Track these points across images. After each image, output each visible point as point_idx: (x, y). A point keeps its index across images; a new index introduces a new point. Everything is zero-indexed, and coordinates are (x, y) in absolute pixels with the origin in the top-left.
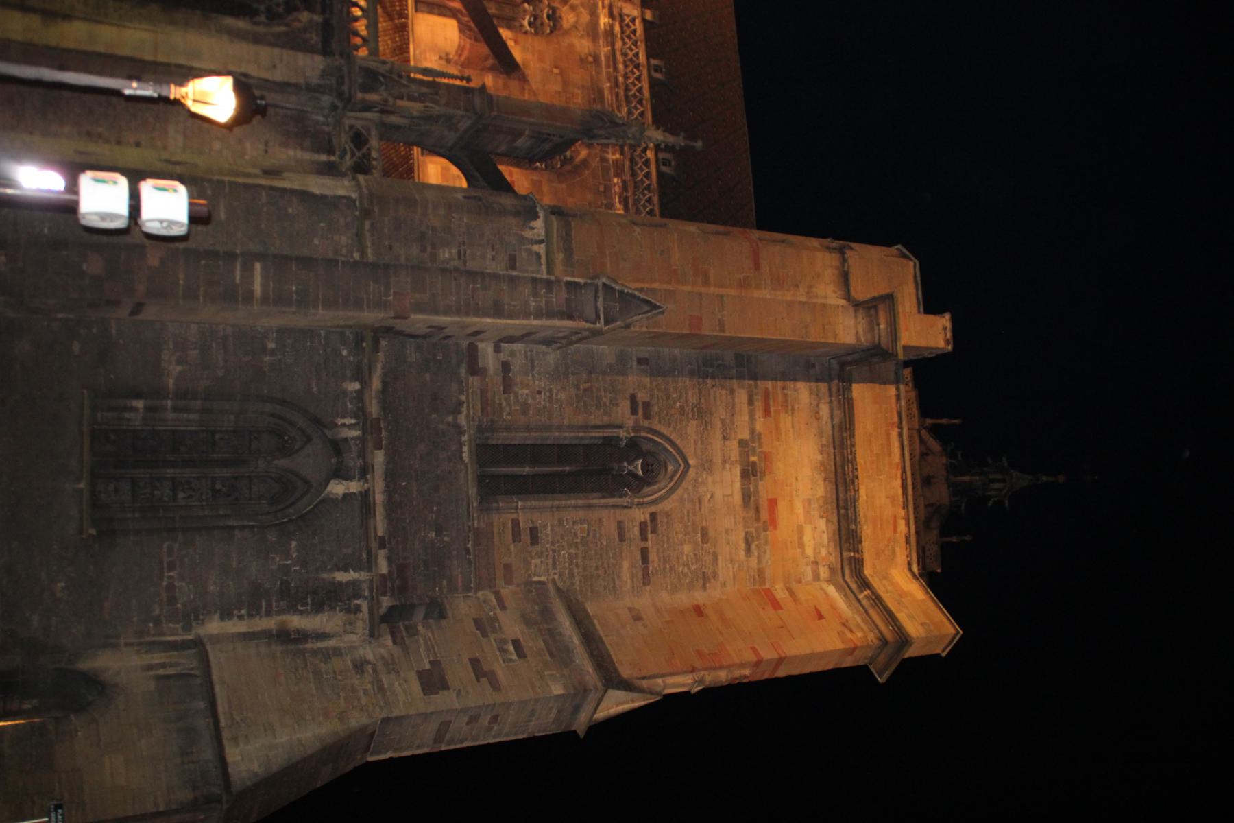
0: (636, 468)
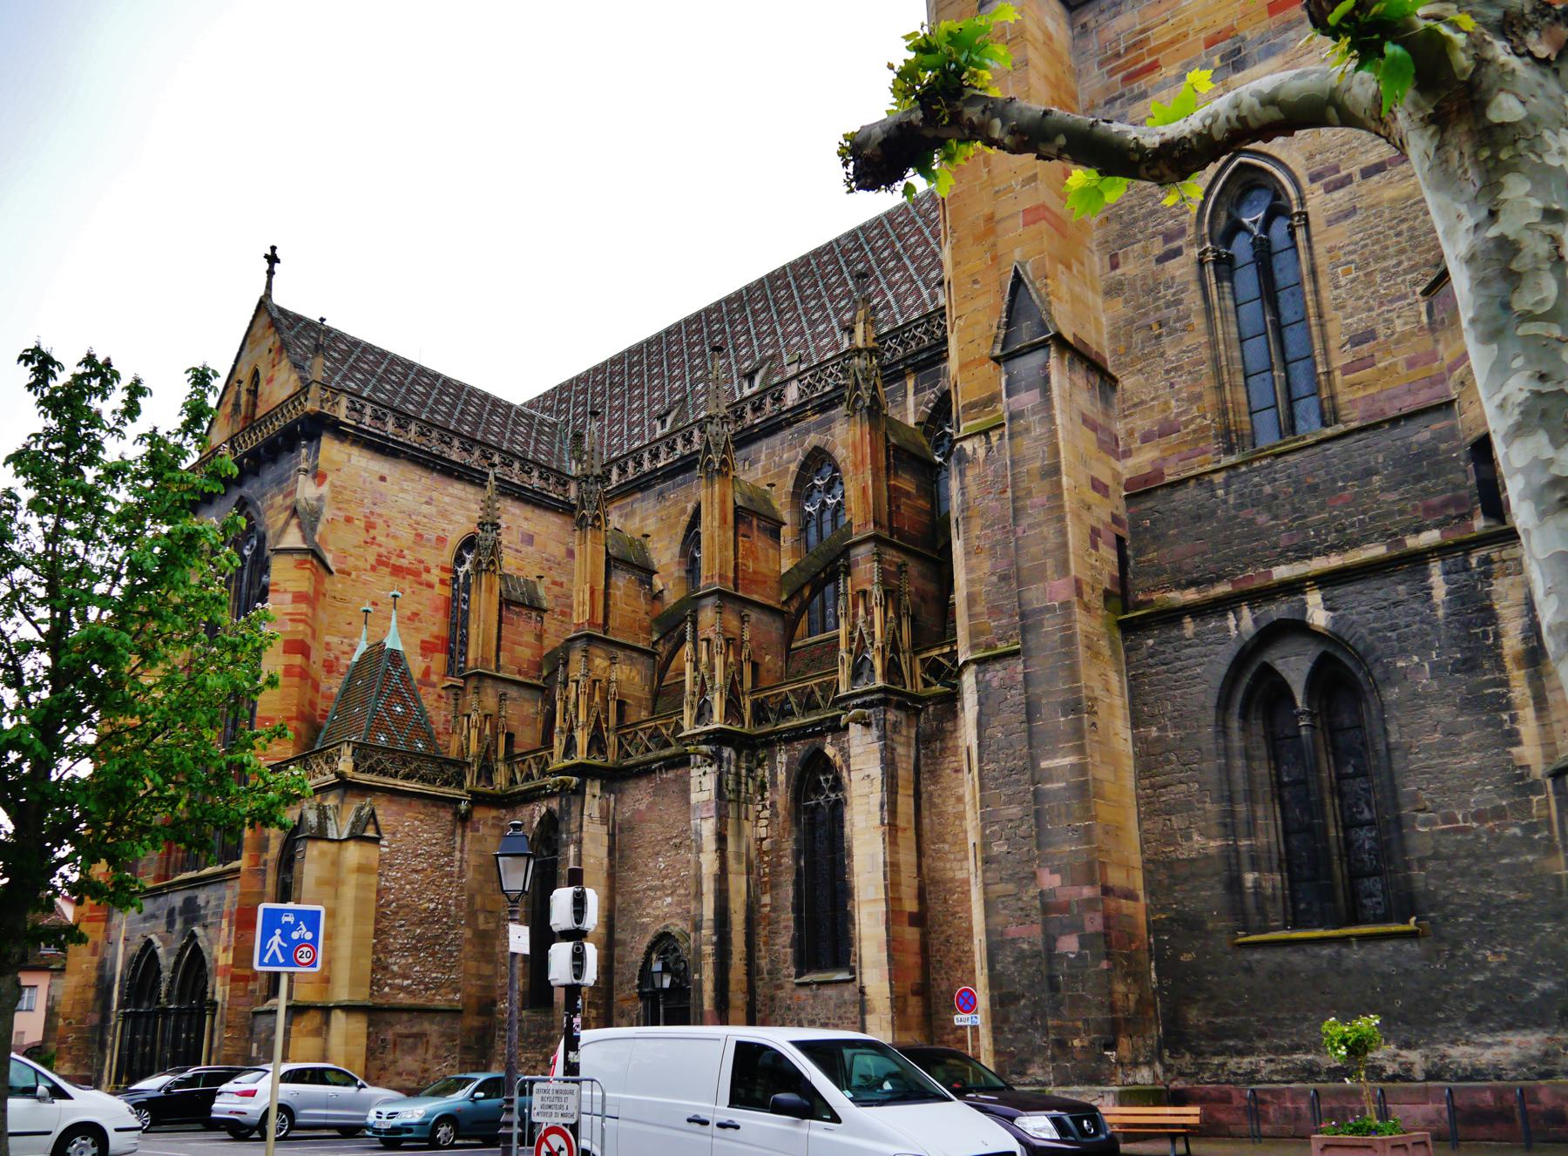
0: (1255, 222)
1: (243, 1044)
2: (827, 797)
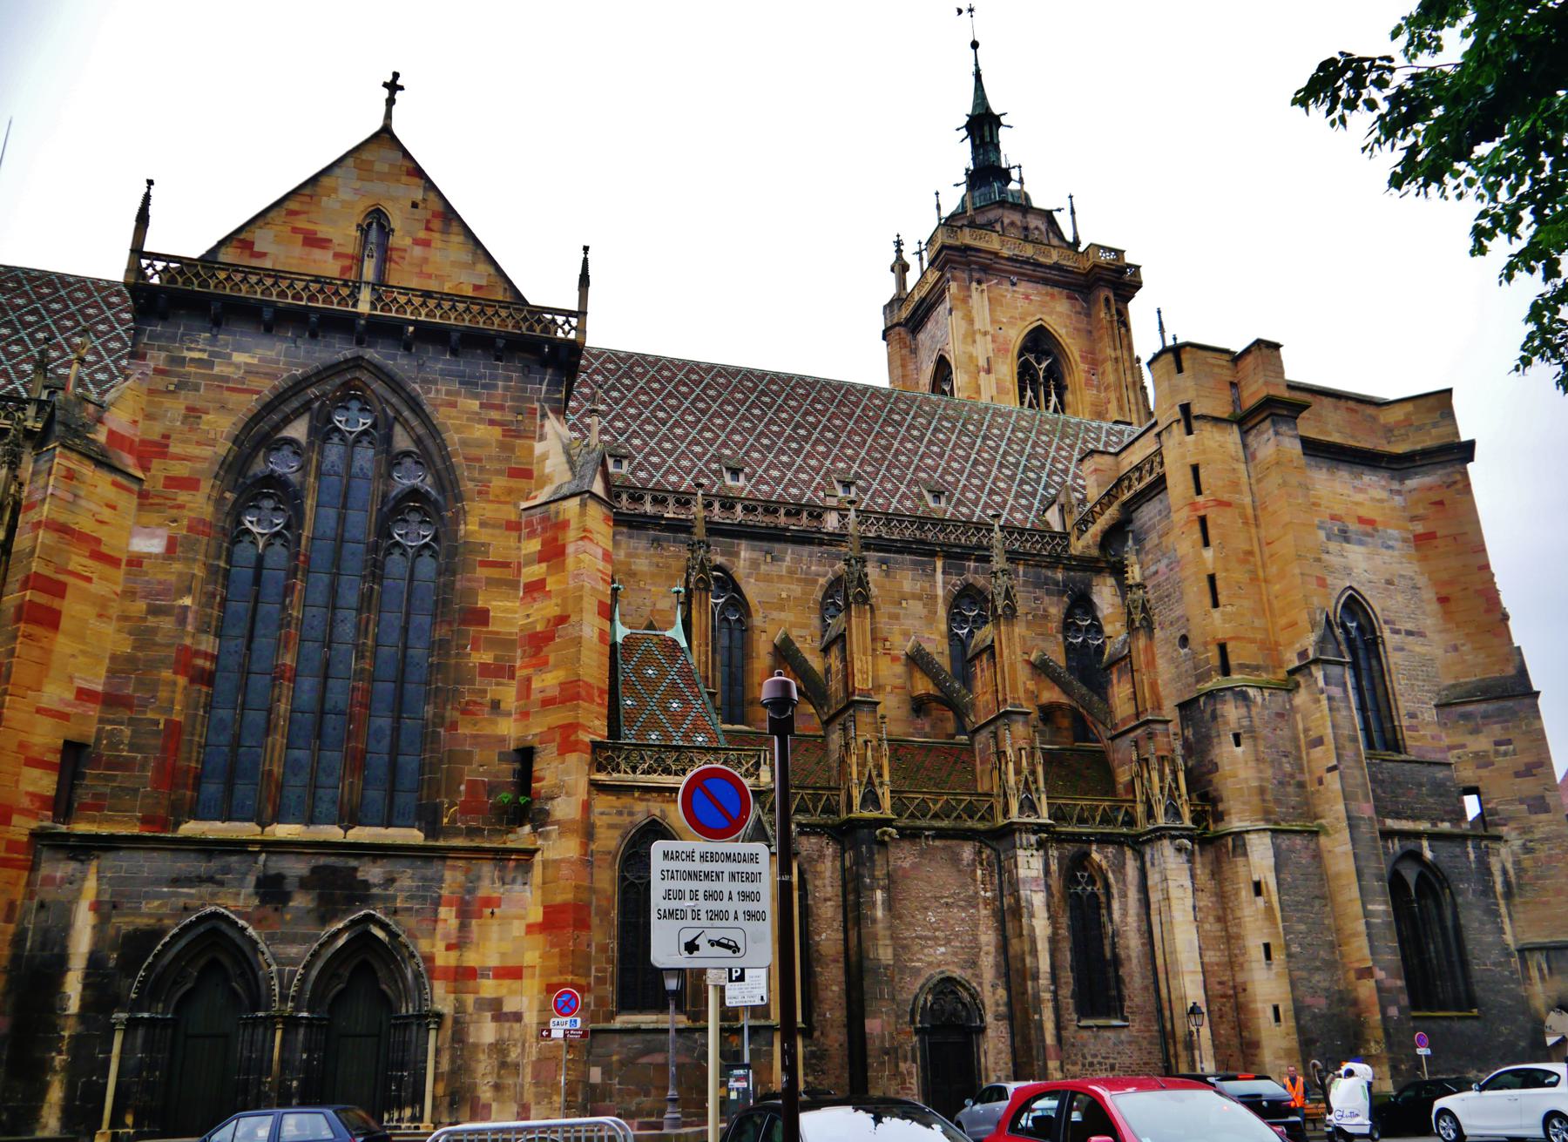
1: (581, 1067)
2: (1084, 889)
